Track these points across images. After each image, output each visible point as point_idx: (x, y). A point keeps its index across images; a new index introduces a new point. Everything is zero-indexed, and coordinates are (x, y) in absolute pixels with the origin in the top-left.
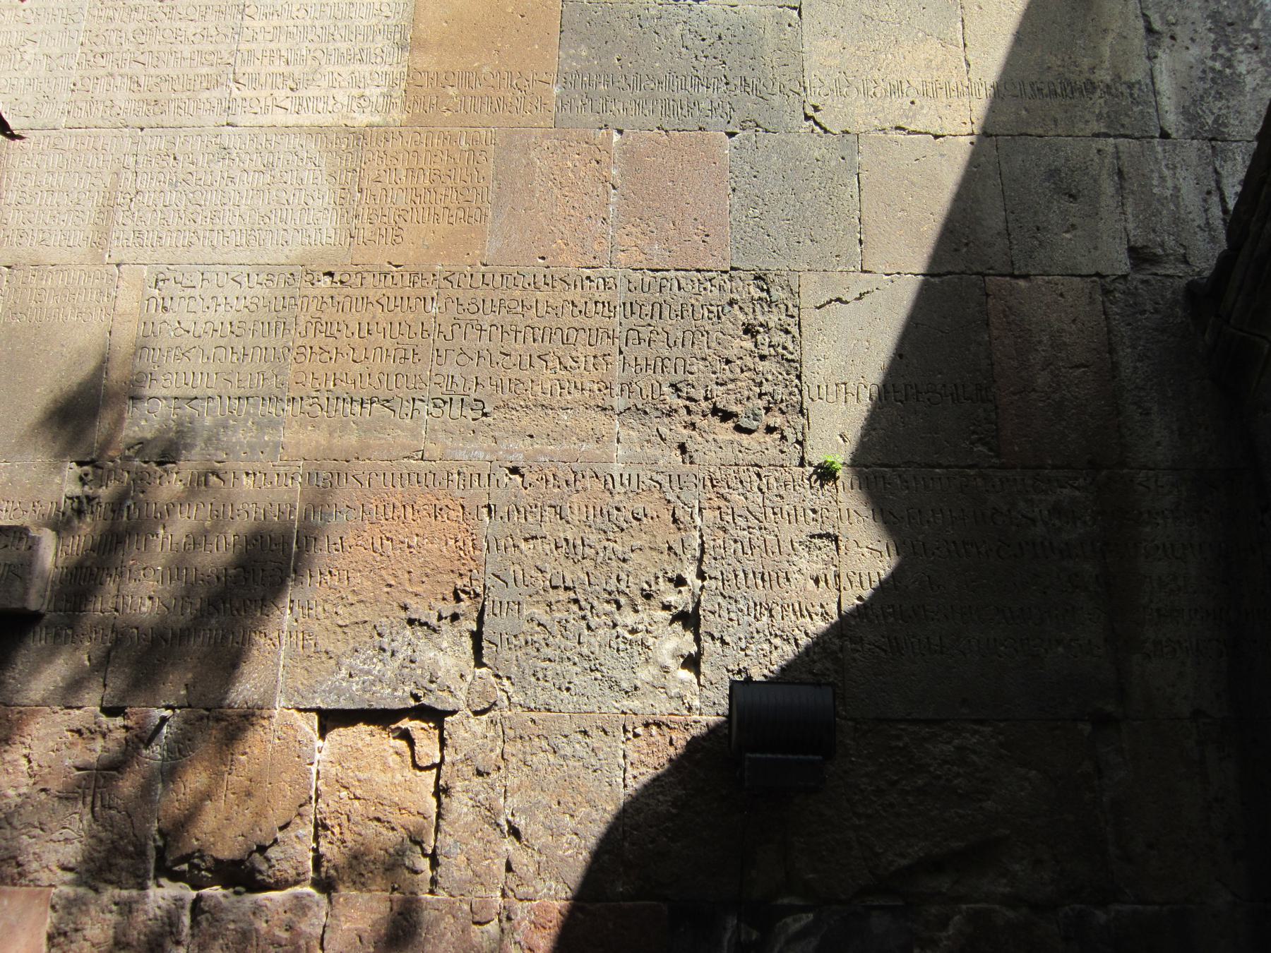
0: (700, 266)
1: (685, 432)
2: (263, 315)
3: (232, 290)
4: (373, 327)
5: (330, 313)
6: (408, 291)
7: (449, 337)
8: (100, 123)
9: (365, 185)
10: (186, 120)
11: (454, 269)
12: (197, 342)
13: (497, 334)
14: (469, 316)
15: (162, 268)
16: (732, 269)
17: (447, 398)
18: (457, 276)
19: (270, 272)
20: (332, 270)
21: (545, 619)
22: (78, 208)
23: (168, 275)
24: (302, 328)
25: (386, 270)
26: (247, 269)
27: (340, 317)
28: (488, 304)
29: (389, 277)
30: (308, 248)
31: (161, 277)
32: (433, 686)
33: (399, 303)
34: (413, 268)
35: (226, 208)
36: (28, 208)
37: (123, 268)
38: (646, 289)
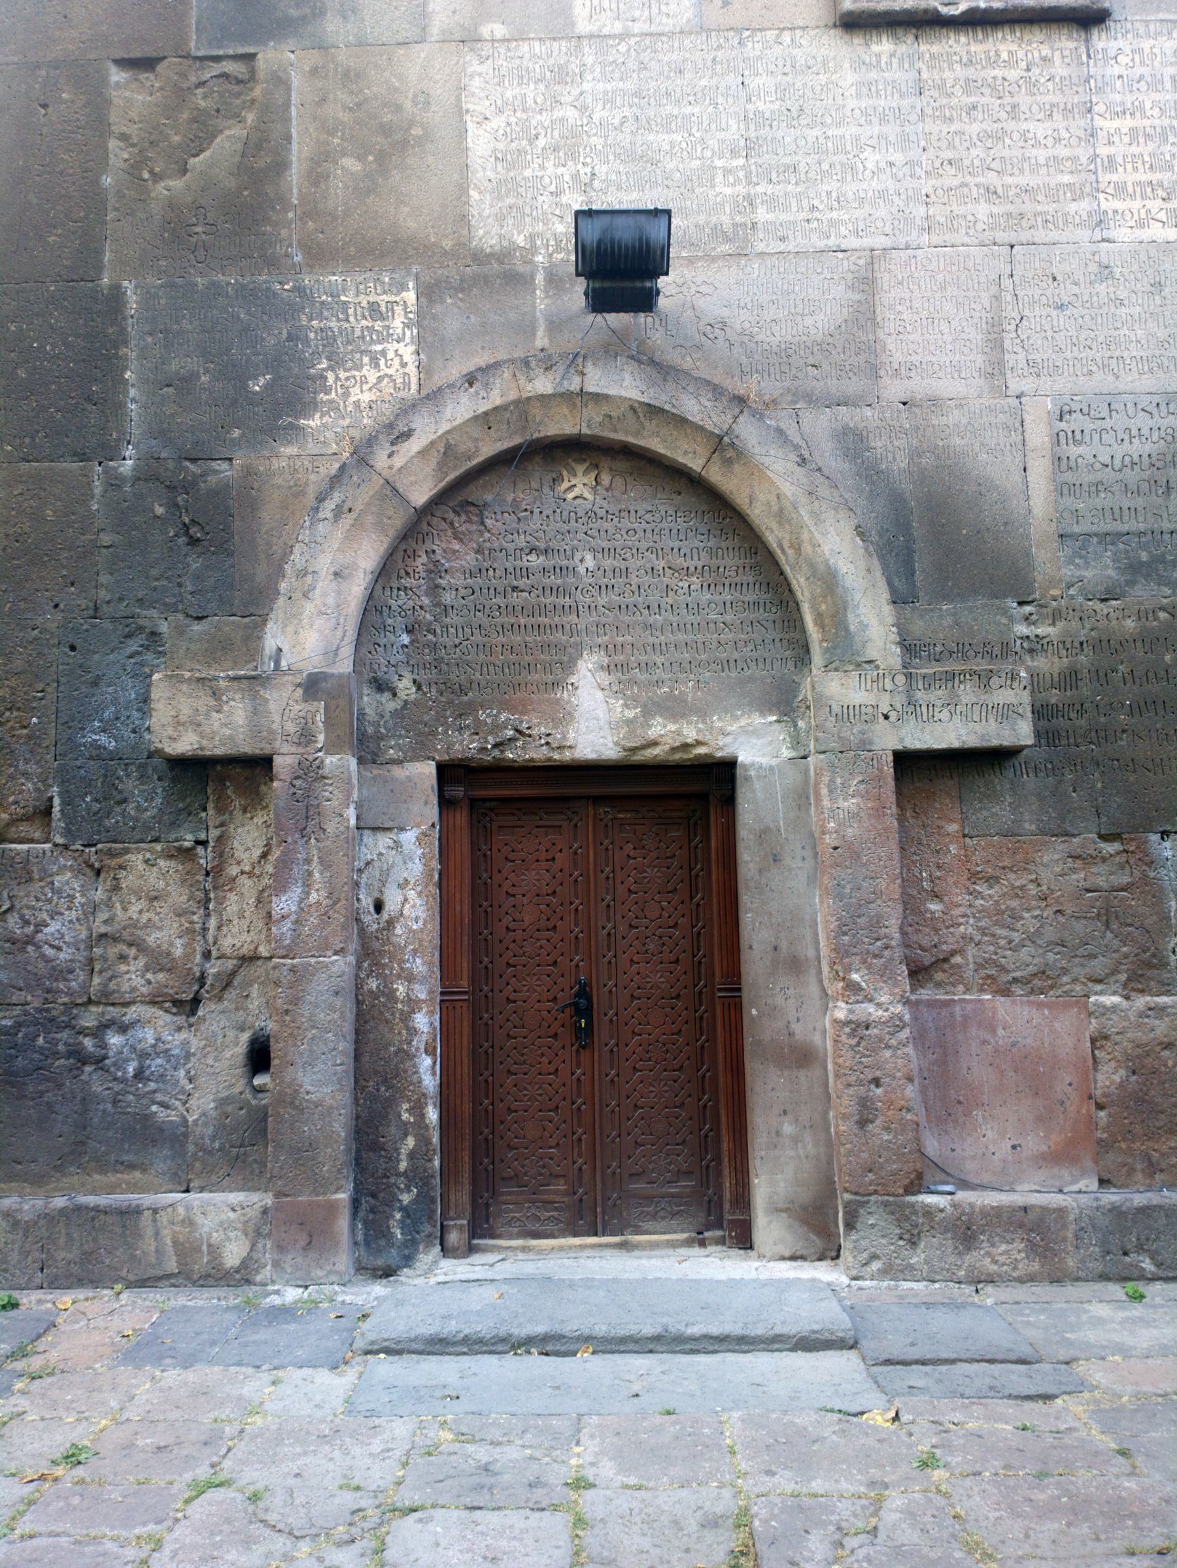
3: (1143, 422)
8: (967, 240)
10: (1055, 235)
12: (1120, 476)
22: (964, 336)
23: (1075, 406)
26: (1156, 399)
31: (1066, 408)
35: (1122, 332)
36: (912, 337)
37: (1024, 400)
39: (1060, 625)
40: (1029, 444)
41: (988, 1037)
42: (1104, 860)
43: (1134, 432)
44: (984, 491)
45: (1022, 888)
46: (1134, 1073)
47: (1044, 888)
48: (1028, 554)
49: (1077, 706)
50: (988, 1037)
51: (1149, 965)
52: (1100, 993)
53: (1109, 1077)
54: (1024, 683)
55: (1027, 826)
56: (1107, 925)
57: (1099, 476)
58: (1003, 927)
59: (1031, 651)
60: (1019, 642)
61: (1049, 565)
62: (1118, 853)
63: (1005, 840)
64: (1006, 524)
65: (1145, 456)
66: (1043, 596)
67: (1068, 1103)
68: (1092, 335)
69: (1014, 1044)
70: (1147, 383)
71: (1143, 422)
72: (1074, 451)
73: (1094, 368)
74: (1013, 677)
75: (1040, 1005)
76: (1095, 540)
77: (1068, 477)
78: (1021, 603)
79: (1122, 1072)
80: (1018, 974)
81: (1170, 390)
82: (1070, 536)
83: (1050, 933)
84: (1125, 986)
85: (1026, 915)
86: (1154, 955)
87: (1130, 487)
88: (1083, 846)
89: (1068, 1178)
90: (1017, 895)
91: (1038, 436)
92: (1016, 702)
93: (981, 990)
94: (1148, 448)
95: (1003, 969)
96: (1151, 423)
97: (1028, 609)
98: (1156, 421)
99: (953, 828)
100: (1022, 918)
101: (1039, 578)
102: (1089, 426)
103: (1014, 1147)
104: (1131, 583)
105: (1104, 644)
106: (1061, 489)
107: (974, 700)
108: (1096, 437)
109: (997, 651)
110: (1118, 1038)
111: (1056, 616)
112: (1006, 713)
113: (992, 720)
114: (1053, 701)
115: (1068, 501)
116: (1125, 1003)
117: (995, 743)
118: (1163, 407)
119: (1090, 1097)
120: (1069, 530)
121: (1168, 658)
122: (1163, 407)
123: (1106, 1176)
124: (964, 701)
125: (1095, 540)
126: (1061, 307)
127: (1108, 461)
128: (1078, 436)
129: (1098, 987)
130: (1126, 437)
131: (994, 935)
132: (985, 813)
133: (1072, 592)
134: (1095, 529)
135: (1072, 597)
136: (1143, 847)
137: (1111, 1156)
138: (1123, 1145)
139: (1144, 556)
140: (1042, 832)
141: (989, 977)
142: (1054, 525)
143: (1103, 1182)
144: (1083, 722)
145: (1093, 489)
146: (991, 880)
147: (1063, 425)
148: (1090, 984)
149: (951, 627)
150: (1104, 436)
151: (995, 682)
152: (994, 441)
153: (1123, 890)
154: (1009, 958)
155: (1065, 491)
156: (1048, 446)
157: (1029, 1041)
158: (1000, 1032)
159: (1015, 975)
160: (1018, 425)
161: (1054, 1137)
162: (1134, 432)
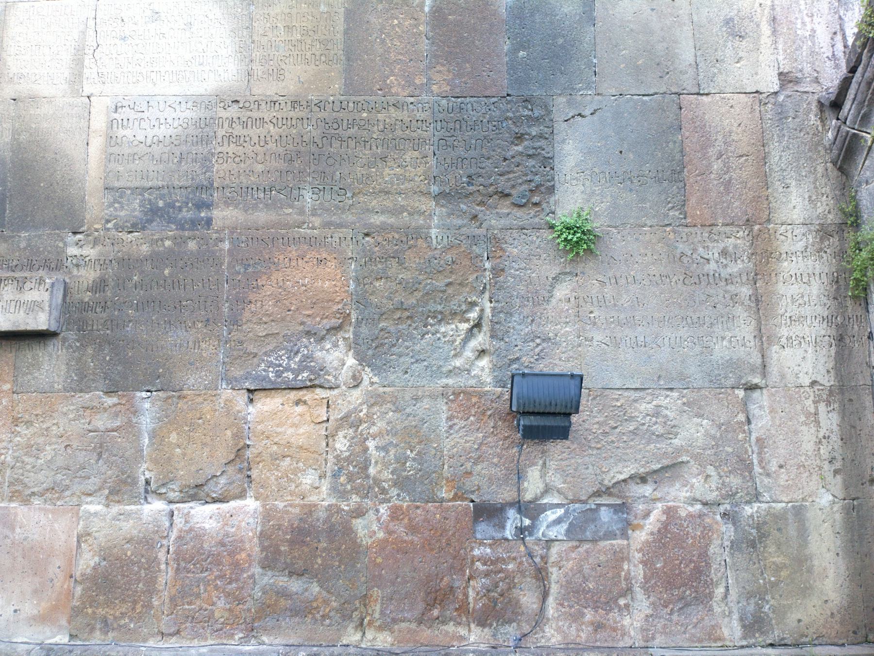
0: (487, 93)
1: (478, 208)
2: (192, 130)
4: (268, 139)
5: (238, 130)
6: (292, 114)
7: (320, 146)
9: (255, 38)
11: (321, 98)
12: (150, 150)
13: (352, 143)
14: (333, 131)
15: (120, 98)
16: (508, 95)
17: (321, 187)
18: (323, 103)
19: (197, 101)
20: (238, 99)
21: (392, 329)
23: (125, 103)
24: (220, 140)
25: (275, 99)
26: (179, 99)
27: (245, 132)
28: (345, 122)
29: (277, 104)
30: (220, 83)
31: (119, 105)
32: (322, 373)
33: (285, 121)
34: (293, 99)
38: (450, 111)
39: (99, 248)
40: (92, 127)
41: (9, 533)
42: (105, 410)
43: (163, 121)
44: (58, 157)
45: (47, 429)
46: (104, 559)
47: (62, 429)
48: (83, 200)
49: (103, 304)
50: (9, 533)
51: (125, 482)
52: (91, 503)
53: (87, 561)
54: (47, 287)
55: (56, 385)
56: (100, 455)
57: (135, 150)
58: (31, 456)
59: (77, 266)
60: (70, 259)
61: (95, 205)
62: (115, 405)
63: (40, 396)
64: (70, 180)
65: (168, 136)
66: (89, 229)
67: (56, 580)
68: (142, 56)
69: (25, 539)
70: (176, 89)
71: (169, 114)
72: (121, 132)
73: (141, 79)
74: (41, 281)
75: (46, 511)
76: (129, 192)
77: (116, 150)
78: (75, 233)
79: (97, 559)
80: (35, 490)
81: (188, 93)
82: (112, 189)
83: (60, 462)
84: (107, 498)
85: (48, 448)
86: (129, 477)
87: (156, 157)
88: (91, 400)
89: (48, 634)
90: (43, 435)
91: (99, 122)
92: (39, 299)
93: (11, 500)
94: (170, 131)
95: (26, 486)
96: (174, 115)
97: (79, 236)
98: (178, 114)
99: (7, 387)
100: (45, 450)
101: (88, 217)
102: (132, 115)
103: (15, 611)
104: (150, 221)
105: (126, 263)
106: (109, 158)
107: (12, 298)
108: (137, 123)
109: (53, 265)
110: (97, 534)
111: (96, 242)
112: (34, 307)
113: (22, 312)
114: (86, 300)
115: (113, 166)
116: (105, 509)
117: (22, 328)
118: (183, 103)
119: (71, 577)
120: (111, 185)
121: (166, 272)
122: (183, 103)
123: (74, 632)
124: (6, 298)
125: (129, 192)
126: (124, 39)
127: (143, 140)
128: (125, 123)
129: (89, 499)
130: (157, 124)
131: (23, 462)
132: (29, 377)
133: (109, 225)
134: (129, 184)
135: (108, 229)
136: (131, 399)
137: (79, 619)
138: (90, 611)
139: (161, 204)
140: (65, 390)
141: (16, 491)
142: (102, 181)
143: (72, 637)
144: (104, 315)
145: (131, 158)
146: (29, 424)
147: (116, 116)
148: (83, 497)
149: (25, 249)
150: (142, 122)
151: (28, 285)
152: (69, 125)
153: (113, 431)
154: (31, 479)
155: (112, 159)
156: (104, 129)
157: (36, 536)
158: (18, 530)
159: (32, 490)
160: (86, 115)
161: (43, 604)
162: (163, 121)
